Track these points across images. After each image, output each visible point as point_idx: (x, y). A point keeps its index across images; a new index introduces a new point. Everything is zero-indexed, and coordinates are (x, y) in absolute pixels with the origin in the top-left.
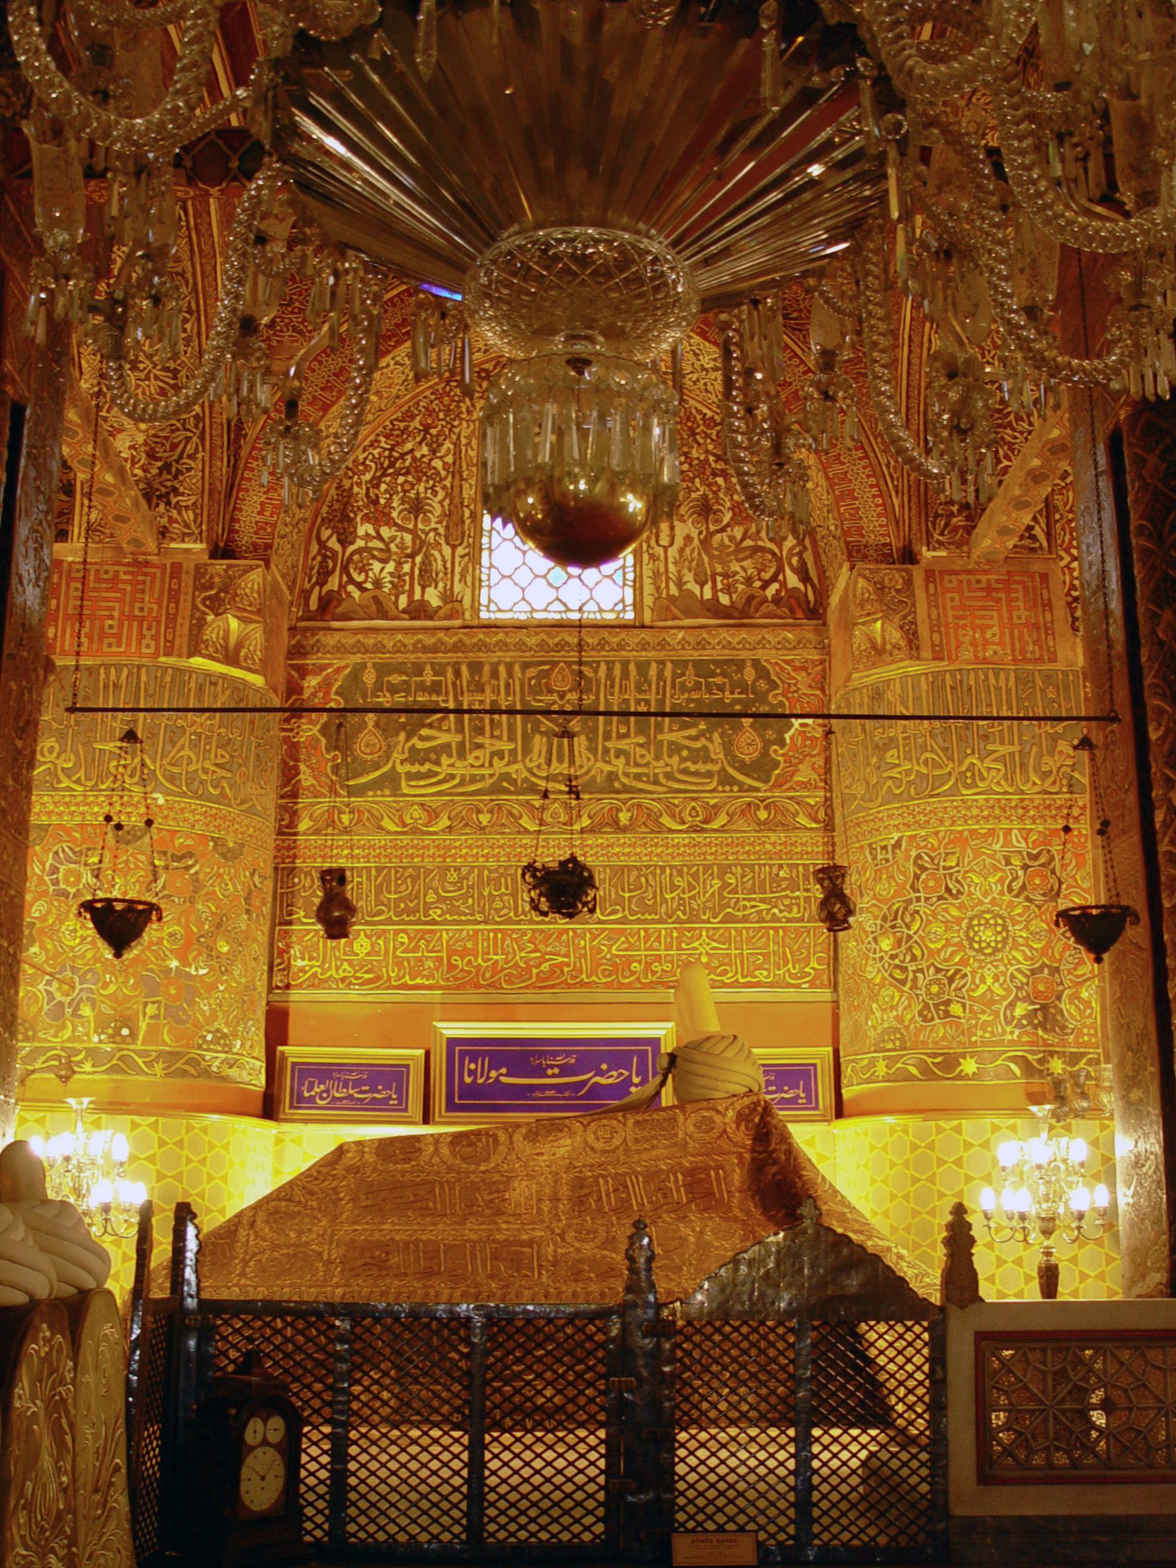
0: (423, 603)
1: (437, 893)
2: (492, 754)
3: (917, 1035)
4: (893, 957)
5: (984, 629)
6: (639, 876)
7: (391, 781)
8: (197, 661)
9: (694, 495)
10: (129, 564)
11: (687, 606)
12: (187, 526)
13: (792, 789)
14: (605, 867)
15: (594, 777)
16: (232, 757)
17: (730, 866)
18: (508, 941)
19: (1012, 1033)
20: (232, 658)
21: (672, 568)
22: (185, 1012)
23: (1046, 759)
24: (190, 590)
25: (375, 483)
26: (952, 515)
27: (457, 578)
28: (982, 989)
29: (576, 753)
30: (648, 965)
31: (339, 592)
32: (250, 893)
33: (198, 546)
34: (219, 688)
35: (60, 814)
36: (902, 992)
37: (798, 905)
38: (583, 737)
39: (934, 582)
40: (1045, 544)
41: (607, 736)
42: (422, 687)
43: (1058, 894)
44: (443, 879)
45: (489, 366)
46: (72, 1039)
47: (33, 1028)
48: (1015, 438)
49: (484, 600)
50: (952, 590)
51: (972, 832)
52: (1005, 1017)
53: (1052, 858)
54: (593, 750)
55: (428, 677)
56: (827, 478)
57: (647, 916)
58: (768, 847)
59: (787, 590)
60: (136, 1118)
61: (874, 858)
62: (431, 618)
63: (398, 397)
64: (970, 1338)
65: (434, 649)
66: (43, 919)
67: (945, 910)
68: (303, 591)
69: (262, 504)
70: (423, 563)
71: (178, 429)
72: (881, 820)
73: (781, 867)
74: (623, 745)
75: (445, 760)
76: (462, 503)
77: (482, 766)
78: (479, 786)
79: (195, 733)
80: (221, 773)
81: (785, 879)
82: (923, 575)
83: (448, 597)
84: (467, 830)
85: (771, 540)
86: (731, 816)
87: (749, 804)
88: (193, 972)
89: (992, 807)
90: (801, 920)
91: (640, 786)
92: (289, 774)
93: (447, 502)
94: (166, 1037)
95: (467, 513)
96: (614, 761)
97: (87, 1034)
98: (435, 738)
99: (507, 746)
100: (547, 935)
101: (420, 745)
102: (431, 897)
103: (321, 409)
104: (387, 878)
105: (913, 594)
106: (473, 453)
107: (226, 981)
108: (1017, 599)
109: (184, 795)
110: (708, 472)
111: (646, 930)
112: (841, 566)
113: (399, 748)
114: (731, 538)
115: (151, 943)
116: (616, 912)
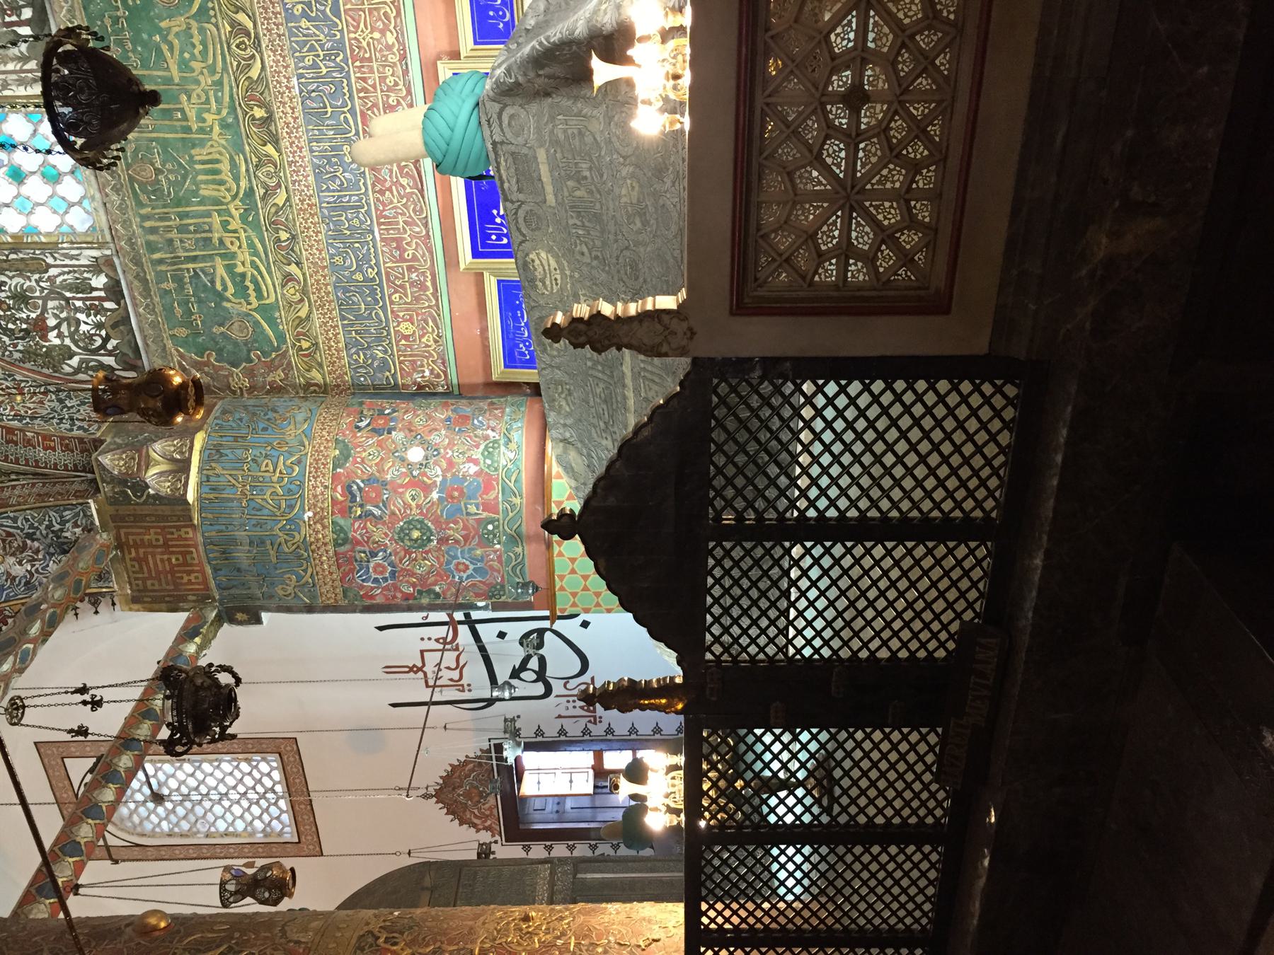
0: (105, 289)
1: (353, 273)
6: (310, 98)
7: (266, 311)
8: (191, 497)
10: (122, 551)
12: (77, 515)
15: (227, 140)
16: (266, 456)
17: (286, 10)
18: (386, 213)
20: (182, 467)
24: (132, 507)
27: (74, 262)
29: (209, 157)
31: (115, 356)
32: (374, 430)
34: (210, 473)
38: (193, 152)
41: (188, 130)
46: (500, 562)
49: (89, 239)
54: (202, 143)
55: (170, 285)
57: (345, 91)
62: (118, 282)
64: (740, 323)
65: (145, 282)
66: (414, 585)
69: (45, 449)
70: (70, 290)
74: (192, 114)
75: (240, 269)
76: (5, 261)
77: (238, 238)
78: (256, 241)
80: (281, 466)
83: (96, 267)
86: (238, 9)
91: (227, 99)
92: (276, 390)
93: (7, 273)
94: (494, 496)
95: (12, 256)
96: (209, 122)
97: (495, 552)
98: (222, 279)
99: (216, 220)
100: (377, 180)
101: (231, 290)
104: (350, 311)
109: (302, 496)
111: (359, 91)
115: (421, 513)
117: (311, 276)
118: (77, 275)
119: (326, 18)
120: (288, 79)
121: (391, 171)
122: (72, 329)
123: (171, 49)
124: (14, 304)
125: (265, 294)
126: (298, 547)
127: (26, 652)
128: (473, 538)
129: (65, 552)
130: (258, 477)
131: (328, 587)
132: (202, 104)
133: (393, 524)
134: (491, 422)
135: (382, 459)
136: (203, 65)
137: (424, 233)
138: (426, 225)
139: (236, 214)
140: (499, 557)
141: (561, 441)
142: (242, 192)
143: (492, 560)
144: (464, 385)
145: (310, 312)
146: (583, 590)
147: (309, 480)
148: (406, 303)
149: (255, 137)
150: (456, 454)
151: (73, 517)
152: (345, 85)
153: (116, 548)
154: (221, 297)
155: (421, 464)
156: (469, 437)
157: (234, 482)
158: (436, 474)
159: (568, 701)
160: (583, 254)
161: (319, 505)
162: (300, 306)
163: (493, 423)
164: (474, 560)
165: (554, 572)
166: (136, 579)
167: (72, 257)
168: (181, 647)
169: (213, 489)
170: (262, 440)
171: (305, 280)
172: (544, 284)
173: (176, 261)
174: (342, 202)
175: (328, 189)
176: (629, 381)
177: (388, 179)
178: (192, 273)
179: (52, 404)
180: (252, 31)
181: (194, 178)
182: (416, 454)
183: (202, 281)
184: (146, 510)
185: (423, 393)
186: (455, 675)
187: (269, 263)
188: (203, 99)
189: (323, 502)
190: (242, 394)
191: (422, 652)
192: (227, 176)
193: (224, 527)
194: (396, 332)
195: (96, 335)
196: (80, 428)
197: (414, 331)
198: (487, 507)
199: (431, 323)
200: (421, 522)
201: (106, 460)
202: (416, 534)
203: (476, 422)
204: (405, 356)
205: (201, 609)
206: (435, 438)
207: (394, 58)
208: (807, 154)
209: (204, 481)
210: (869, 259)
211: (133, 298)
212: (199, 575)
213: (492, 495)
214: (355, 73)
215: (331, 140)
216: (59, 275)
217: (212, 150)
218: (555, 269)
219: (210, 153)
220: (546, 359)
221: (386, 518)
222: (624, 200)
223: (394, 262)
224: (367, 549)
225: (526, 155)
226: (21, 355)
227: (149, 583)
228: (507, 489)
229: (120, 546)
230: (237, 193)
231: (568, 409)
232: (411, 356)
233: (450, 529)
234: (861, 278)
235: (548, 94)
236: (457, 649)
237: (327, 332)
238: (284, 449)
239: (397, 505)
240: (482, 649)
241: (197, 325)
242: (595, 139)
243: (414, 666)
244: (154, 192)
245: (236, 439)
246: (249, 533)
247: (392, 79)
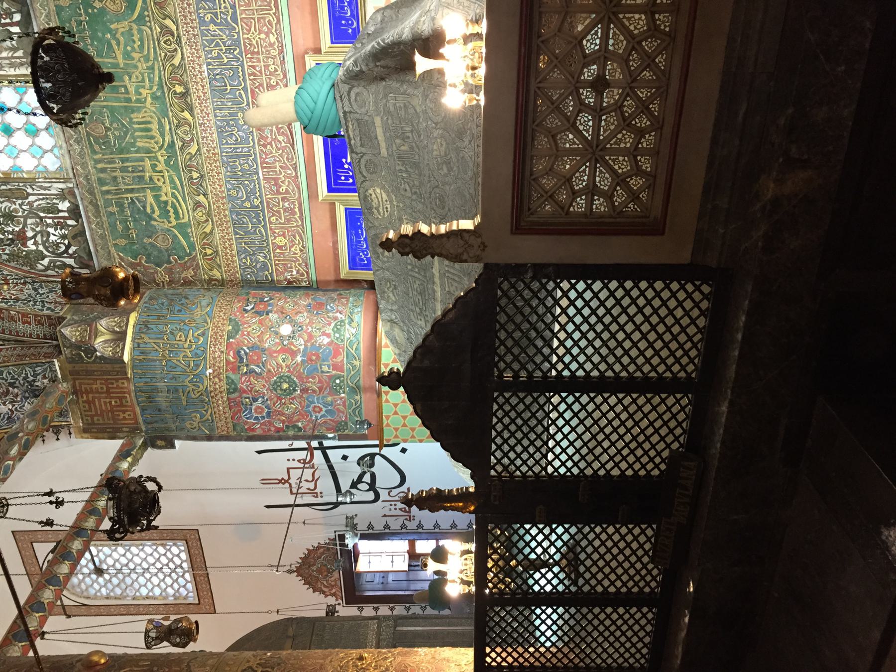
0: (69, 210)
1: (244, 202)
6: (215, 79)
7: (182, 228)
8: (126, 358)
10: (77, 396)
14: (213, 102)
15: (156, 108)
16: (180, 330)
17: (200, 18)
20: (121, 337)
29: (144, 120)
30: (271, 74)
31: (75, 258)
32: (256, 312)
34: (140, 341)
38: (132, 116)
41: (129, 100)
42: (123, 211)
44: (237, 198)
46: (344, 406)
47: (340, 423)
49: (58, 176)
54: (139, 110)
57: (240, 74)
62: (78, 206)
65: (96, 206)
66: (283, 422)
69: (24, 323)
70: (44, 212)
74: (132, 89)
75: (164, 198)
77: (163, 177)
78: (176, 179)
79: (169, 354)
80: (190, 337)
83: (62, 196)
84: (204, 184)
86: (166, 17)
88: (303, 347)
91: (157, 79)
92: (188, 283)
94: (339, 361)
97: (341, 399)
99: (148, 163)
100: (262, 137)
101: (157, 213)
104: (241, 228)
109: (205, 358)
111: (250, 75)
113: (161, 224)
115: (289, 371)
117: (214, 204)
119: (228, 24)
120: (200, 66)
121: (271, 131)
122: (44, 239)
123: (118, 44)
124: (4, 221)
125: (181, 216)
126: (202, 394)
127: (8, 466)
128: (325, 389)
129: (36, 396)
130: (173, 345)
131: (223, 422)
132: (139, 82)
133: (269, 379)
134: (339, 307)
135: (262, 332)
136: (141, 55)
137: (294, 174)
138: (295, 169)
139: (162, 159)
140: (344, 403)
141: (389, 321)
143: (339, 405)
144: (320, 281)
145: (213, 229)
146: (403, 426)
147: (210, 347)
148: (280, 223)
149: (176, 106)
150: (314, 330)
151: (43, 372)
152: (240, 70)
153: (73, 393)
154: (150, 218)
155: (290, 337)
156: (324, 318)
157: (157, 347)
158: (300, 343)
159: (391, 505)
160: (406, 190)
161: (217, 364)
162: (205, 225)
163: (340, 308)
164: (326, 404)
165: (382, 414)
166: (86, 415)
167: (45, 189)
168: (117, 464)
169: (142, 353)
170: (178, 319)
172: (378, 211)
173: (118, 192)
174: (236, 152)
175: (227, 143)
177: (270, 136)
178: (130, 201)
179: (29, 292)
180: (175, 32)
181: (132, 134)
182: (286, 330)
183: (137, 206)
184: (95, 367)
185: (291, 287)
186: (312, 485)
187: (184, 194)
188: (140, 79)
189: (219, 363)
191: (288, 469)
192: (155, 133)
193: (149, 380)
194: (273, 243)
195: (61, 243)
196: (48, 309)
197: (286, 243)
199: (298, 238)
200: (289, 377)
201: (67, 331)
202: (285, 386)
203: (328, 307)
204: (279, 260)
205: (132, 438)
206: (299, 318)
207: (275, 53)
208: (566, 122)
209: (136, 346)
210: (609, 197)
211: (88, 217)
212: (132, 413)
213: (339, 359)
214: (247, 62)
216: (36, 200)
217: (146, 115)
218: (386, 201)
219: (144, 117)
220: (379, 263)
221: (264, 374)
222: (435, 153)
223: (272, 195)
224: (251, 396)
225: (367, 121)
227: (95, 418)
228: (350, 354)
229: (75, 392)
230: (163, 145)
231: (394, 299)
232: (283, 260)
234: (603, 209)
235: (383, 79)
236: (313, 467)
237: (224, 243)
238: (192, 325)
239: (272, 365)
240: (331, 467)
241: (133, 237)
242: (415, 110)
243: (283, 479)
245: (159, 317)
247: (273, 67)
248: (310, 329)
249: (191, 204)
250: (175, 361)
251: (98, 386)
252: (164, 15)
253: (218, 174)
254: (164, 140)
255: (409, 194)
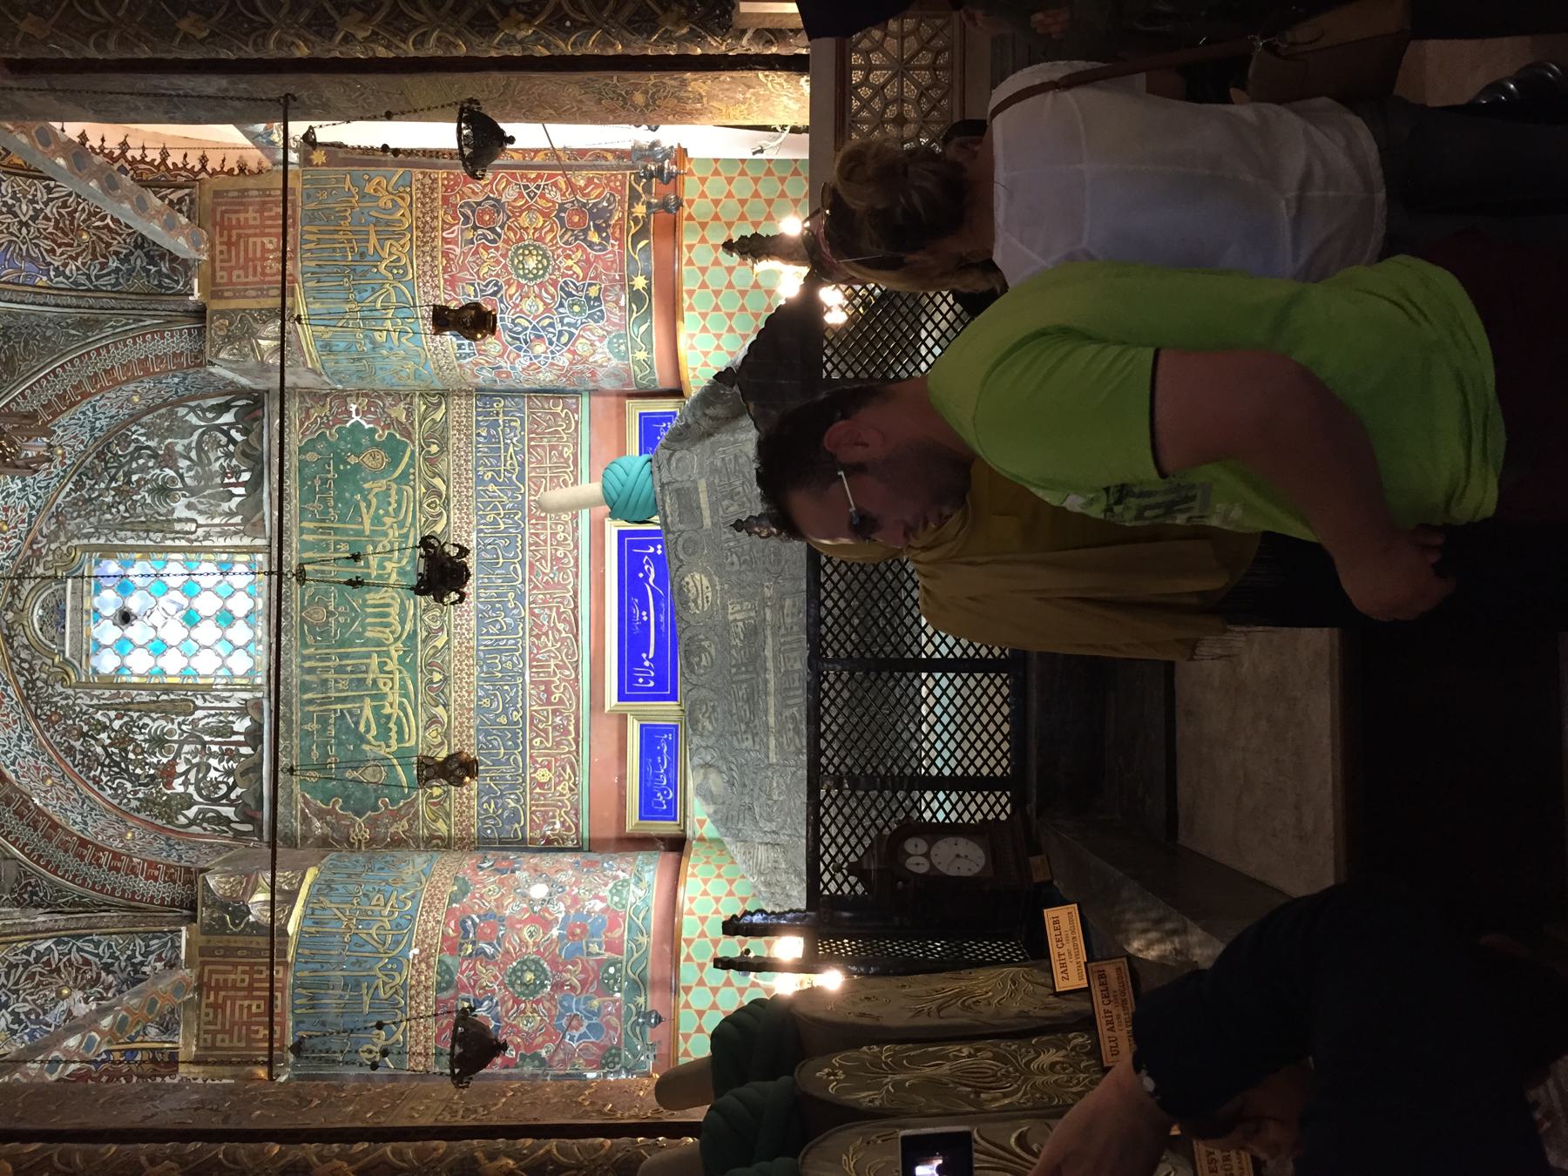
0: (247, 733)
1: (498, 716)
2: (382, 671)
3: (615, 324)
4: (551, 343)
5: (264, 250)
6: (485, 550)
8: (292, 928)
9: (149, 501)
10: (200, 995)
11: (251, 507)
12: (165, 944)
13: (412, 424)
17: (478, 476)
19: (613, 245)
21: (217, 521)
22: (595, 919)
23: (381, 204)
24: (226, 937)
25: (134, 779)
26: (159, 272)
27: (224, 704)
28: (577, 269)
29: (382, 601)
30: (559, 544)
31: (236, 806)
33: (184, 934)
34: (316, 906)
35: (427, 1039)
36: (579, 336)
37: (511, 421)
38: (367, 596)
39: (222, 291)
40: (187, 191)
42: (324, 729)
43: (498, 201)
44: (489, 710)
45: (21, 680)
46: (618, 1016)
48: (83, 209)
49: (244, 682)
50: (230, 276)
51: (445, 270)
52: (600, 250)
53: (467, 204)
56: (127, 382)
58: (462, 445)
59: (237, 423)
60: (682, 958)
61: (469, 355)
62: (261, 726)
63: (50, 761)
67: (511, 296)
68: (234, 838)
69: (147, 878)
70: (210, 734)
71: (69, 960)
72: (436, 348)
73: (478, 435)
75: (387, 710)
76: (154, 702)
77: (392, 679)
78: (409, 682)
81: (488, 432)
82: (215, 301)
83: (242, 712)
85: (191, 435)
86: (435, 475)
87: (425, 459)
88: (563, 914)
89: (424, 252)
90: (522, 419)
93: (154, 715)
95: (164, 697)
97: (615, 1002)
98: (368, 720)
99: (375, 660)
101: (374, 732)
102: (503, 720)
103: (55, 830)
105: (233, 311)
106: (107, 693)
107: (571, 886)
108: (238, 220)
109: (411, 931)
110: (126, 488)
112: (211, 374)
113: (376, 749)
114: (189, 469)
116: (515, 569)
118: (222, 718)
119: (512, 483)
120: (469, 534)
121: (550, 616)
123: (369, 506)
126: (396, 992)
133: (505, 964)
138: (576, 669)
139: (395, 655)
140: (618, 1010)
141: (702, 766)
142: (404, 638)
143: (610, 1014)
147: (422, 915)
148: (546, 748)
151: (160, 948)
154: (362, 739)
158: (559, 910)
160: (733, 564)
161: (428, 941)
163: (623, 866)
164: (592, 1014)
166: (206, 1032)
167: (222, 700)
171: (449, 722)
172: (696, 604)
175: (488, 633)
176: (770, 665)
181: (363, 620)
182: (539, 891)
184: (240, 941)
187: (416, 705)
189: (432, 938)
190: (360, 847)
192: (394, 619)
193: (319, 966)
194: (532, 779)
198: (612, 946)
199: (568, 770)
200: (536, 962)
202: (529, 976)
204: (537, 806)
206: (561, 877)
213: (617, 933)
215: (498, 587)
216: (205, 717)
220: (694, 679)
221: (499, 958)
224: (472, 997)
226: (138, 803)
227: (219, 1037)
229: (198, 989)
231: (711, 729)
232: (543, 805)
233: (568, 971)
235: (710, 435)
244: (320, 634)
246: (345, 973)
248: (576, 890)
249: (423, 717)
250: (364, 936)
251: (239, 977)
252: (434, 473)
253: (469, 675)
254: (403, 628)
255: (736, 567)
